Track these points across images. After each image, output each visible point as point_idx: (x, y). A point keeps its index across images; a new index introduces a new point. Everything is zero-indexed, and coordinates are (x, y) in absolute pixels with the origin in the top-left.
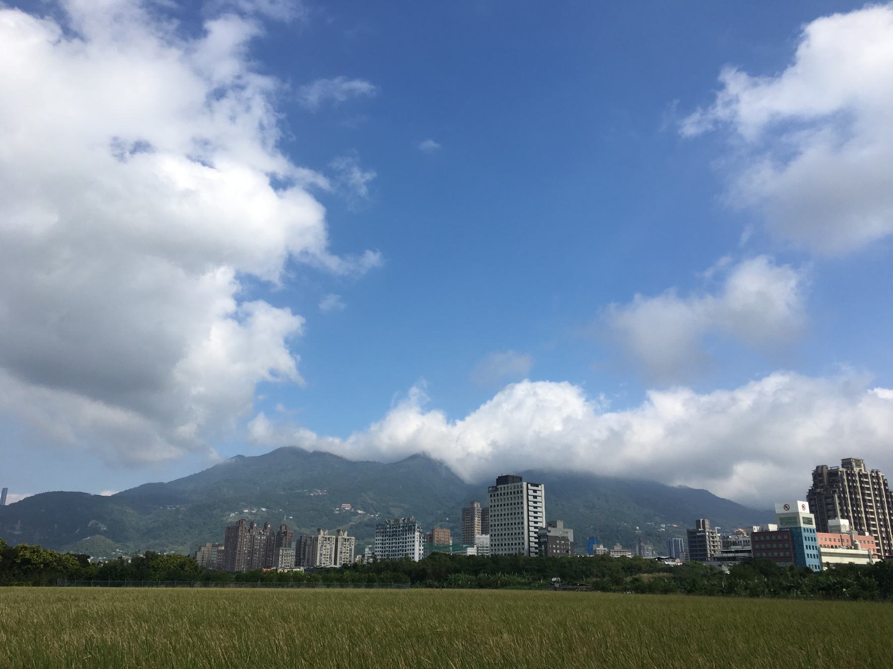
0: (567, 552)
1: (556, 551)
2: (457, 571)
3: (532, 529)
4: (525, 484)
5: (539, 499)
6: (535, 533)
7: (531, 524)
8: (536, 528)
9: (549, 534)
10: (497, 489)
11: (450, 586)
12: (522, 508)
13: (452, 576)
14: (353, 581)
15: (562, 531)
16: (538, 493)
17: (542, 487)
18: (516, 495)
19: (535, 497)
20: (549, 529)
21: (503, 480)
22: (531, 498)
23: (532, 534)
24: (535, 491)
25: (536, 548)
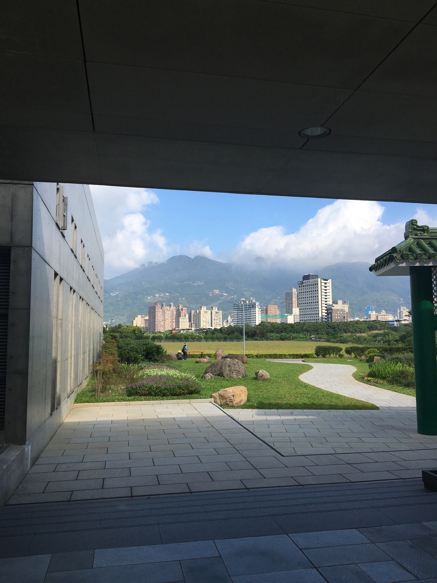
0: (344, 318)
1: (336, 318)
2: (272, 332)
3: (323, 305)
4: (319, 279)
5: (328, 288)
6: (326, 307)
7: (323, 302)
8: (326, 304)
9: (332, 308)
10: (303, 283)
11: (267, 339)
12: (318, 293)
13: (269, 334)
14: (217, 339)
15: (341, 307)
16: (327, 285)
17: (330, 281)
18: (314, 286)
19: (326, 287)
20: (333, 305)
21: (306, 277)
22: (323, 288)
23: (323, 308)
24: (325, 283)
25: (326, 316)
